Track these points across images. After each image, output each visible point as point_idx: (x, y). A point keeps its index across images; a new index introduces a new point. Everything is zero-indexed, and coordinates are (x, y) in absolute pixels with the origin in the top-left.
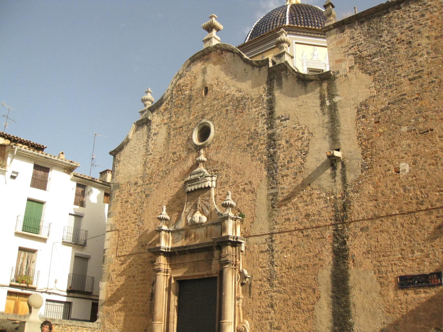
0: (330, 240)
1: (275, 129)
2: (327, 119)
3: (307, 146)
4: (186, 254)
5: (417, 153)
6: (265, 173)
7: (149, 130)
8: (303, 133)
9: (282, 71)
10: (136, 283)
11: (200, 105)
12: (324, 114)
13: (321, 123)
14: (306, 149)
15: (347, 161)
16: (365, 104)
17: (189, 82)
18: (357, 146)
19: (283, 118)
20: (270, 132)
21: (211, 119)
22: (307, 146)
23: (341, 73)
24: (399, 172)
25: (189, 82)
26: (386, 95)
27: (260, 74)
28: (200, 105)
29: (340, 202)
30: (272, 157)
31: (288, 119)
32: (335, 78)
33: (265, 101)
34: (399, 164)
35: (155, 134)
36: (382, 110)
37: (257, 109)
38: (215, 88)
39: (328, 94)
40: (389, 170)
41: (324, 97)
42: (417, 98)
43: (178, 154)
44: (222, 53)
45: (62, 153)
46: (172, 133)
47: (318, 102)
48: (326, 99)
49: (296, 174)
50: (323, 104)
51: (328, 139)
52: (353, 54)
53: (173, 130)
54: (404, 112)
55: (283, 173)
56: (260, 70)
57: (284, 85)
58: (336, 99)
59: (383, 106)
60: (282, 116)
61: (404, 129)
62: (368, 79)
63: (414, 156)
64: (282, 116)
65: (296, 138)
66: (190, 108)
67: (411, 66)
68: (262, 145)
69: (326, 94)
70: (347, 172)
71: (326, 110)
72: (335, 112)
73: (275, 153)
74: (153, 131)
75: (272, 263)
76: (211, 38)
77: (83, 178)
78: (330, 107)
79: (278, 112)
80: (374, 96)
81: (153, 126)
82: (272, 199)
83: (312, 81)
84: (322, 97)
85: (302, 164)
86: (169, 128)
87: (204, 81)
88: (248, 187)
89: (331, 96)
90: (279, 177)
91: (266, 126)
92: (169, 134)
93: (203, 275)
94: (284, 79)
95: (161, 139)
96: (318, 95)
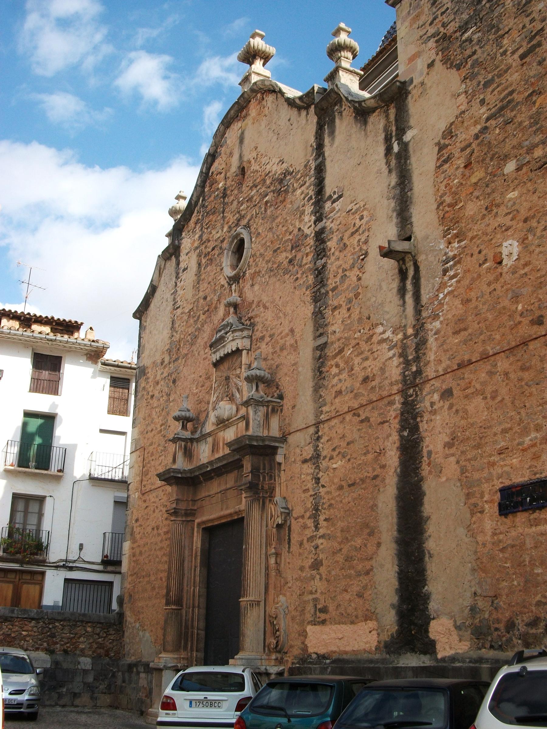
0: (395, 424)
1: (324, 221)
2: (394, 179)
3: (366, 242)
4: (212, 478)
5: (531, 213)
6: (311, 308)
7: (178, 264)
8: (361, 218)
9: (336, 104)
10: (160, 538)
11: (235, 203)
12: (390, 171)
13: (386, 190)
14: (365, 247)
15: (421, 258)
16: (449, 133)
17: (224, 166)
18: (436, 222)
19: (335, 196)
20: (320, 225)
21: (247, 226)
22: (366, 242)
23: (415, 82)
24: (500, 263)
25: (224, 166)
26: (482, 102)
27: (307, 120)
28: (235, 203)
29: (411, 343)
30: (320, 273)
31: (340, 197)
32: (407, 93)
33: (312, 172)
34: (501, 245)
35: (184, 270)
36: (477, 137)
37: (303, 188)
38: (255, 167)
39: (397, 129)
40: (486, 260)
41: (391, 137)
42: (531, 95)
43: (208, 299)
44: (263, 99)
45: (91, 328)
46: (204, 261)
47: (382, 150)
48: (394, 139)
49: (350, 301)
50: (389, 150)
51: (395, 220)
52: (433, 36)
53: (207, 258)
54: (509, 128)
55: (335, 303)
56: (308, 114)
57: (337, 133)
58: (408, 136)
59: (479, 127)
60: (335, 193)
61: (510, 167)
62: (454, 79)
63: (525, 221)
64: (335, 193)
65: (352, 230)
66: (223, 213)
67: (524, 27)
68: (307, 255)
69: (394, 128)
70: (423, 281)
71: (393, 162)
72: (405, 162)
73: (324, 266)
74: (182, 265)
75: (317, 480)
76: (250, 75)
77: (118, 366)
78: (399, 156)
79: (330, 186)
80: (464, 112)
81: (183, 257)
82: (320, 357)
83: (373, 110)
84: (388, 140)
85: (359, 279)
86: (199, 255)
87: (241, 157)
88: (290, 341)
89: (401, 131)
90: (328, 312)
91: (313, 218)
92: (199, 265)
93: (231, 515)
94: (337, 121)
95: (189, 278)
96: (383, 136)
